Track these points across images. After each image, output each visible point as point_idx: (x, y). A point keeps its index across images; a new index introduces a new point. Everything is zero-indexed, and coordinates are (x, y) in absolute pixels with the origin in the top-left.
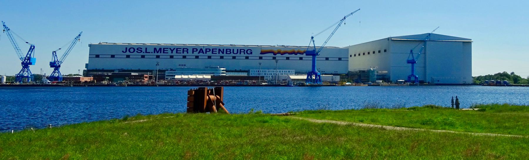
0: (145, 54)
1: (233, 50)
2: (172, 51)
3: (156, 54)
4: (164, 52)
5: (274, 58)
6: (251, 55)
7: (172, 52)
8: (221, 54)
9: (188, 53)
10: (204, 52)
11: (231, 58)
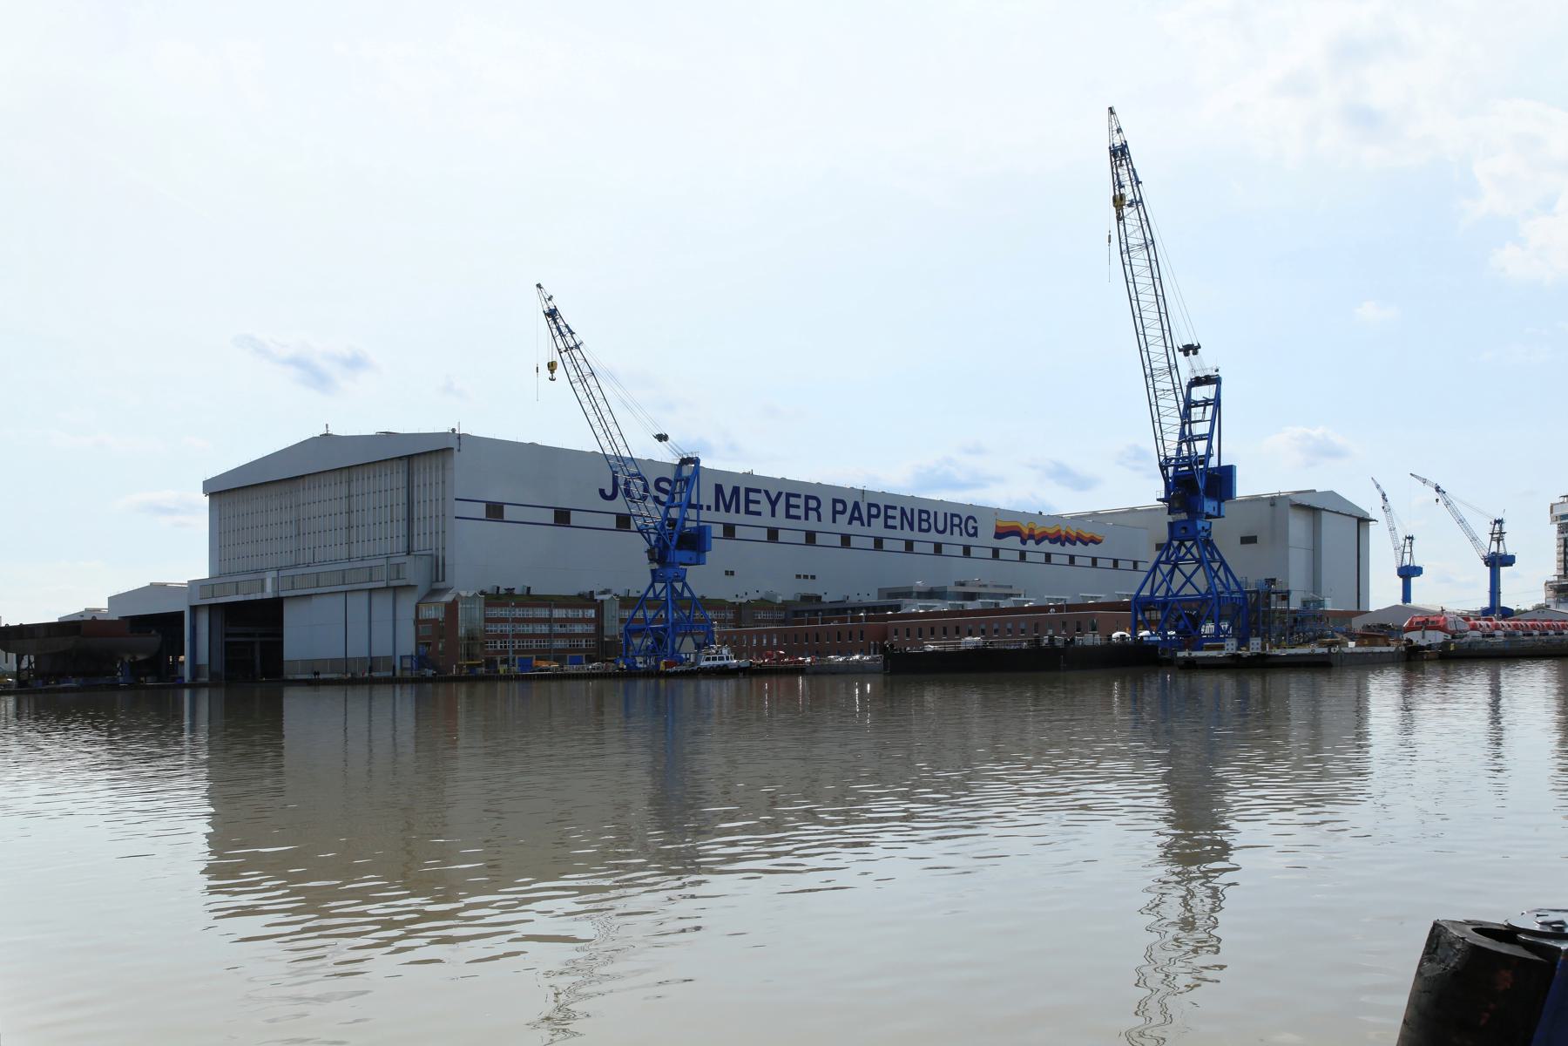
2: (773, 504)
7: (773, 515)
8: (907, 534)
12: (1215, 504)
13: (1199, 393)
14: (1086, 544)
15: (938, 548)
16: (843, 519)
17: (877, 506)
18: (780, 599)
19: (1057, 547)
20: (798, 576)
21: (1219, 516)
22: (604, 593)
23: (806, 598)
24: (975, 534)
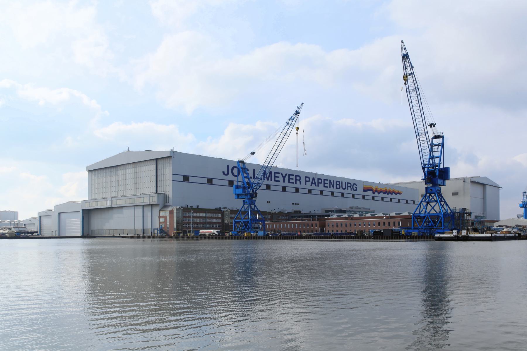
2: (284, 178)
4: (275, 180)
7: (284, 182)
9: (300, 184)
12: (442, 181)
13: (437, 141)
14: (396, 194)
15: (343, 195)
16: (309, 184)
17: (321, 179)
18: (286, 212)
19: (385, 195)
20: (293, 204)
21: (444, 185)
22: (224, 208)
23: (296, 212)
24: (356, 190)
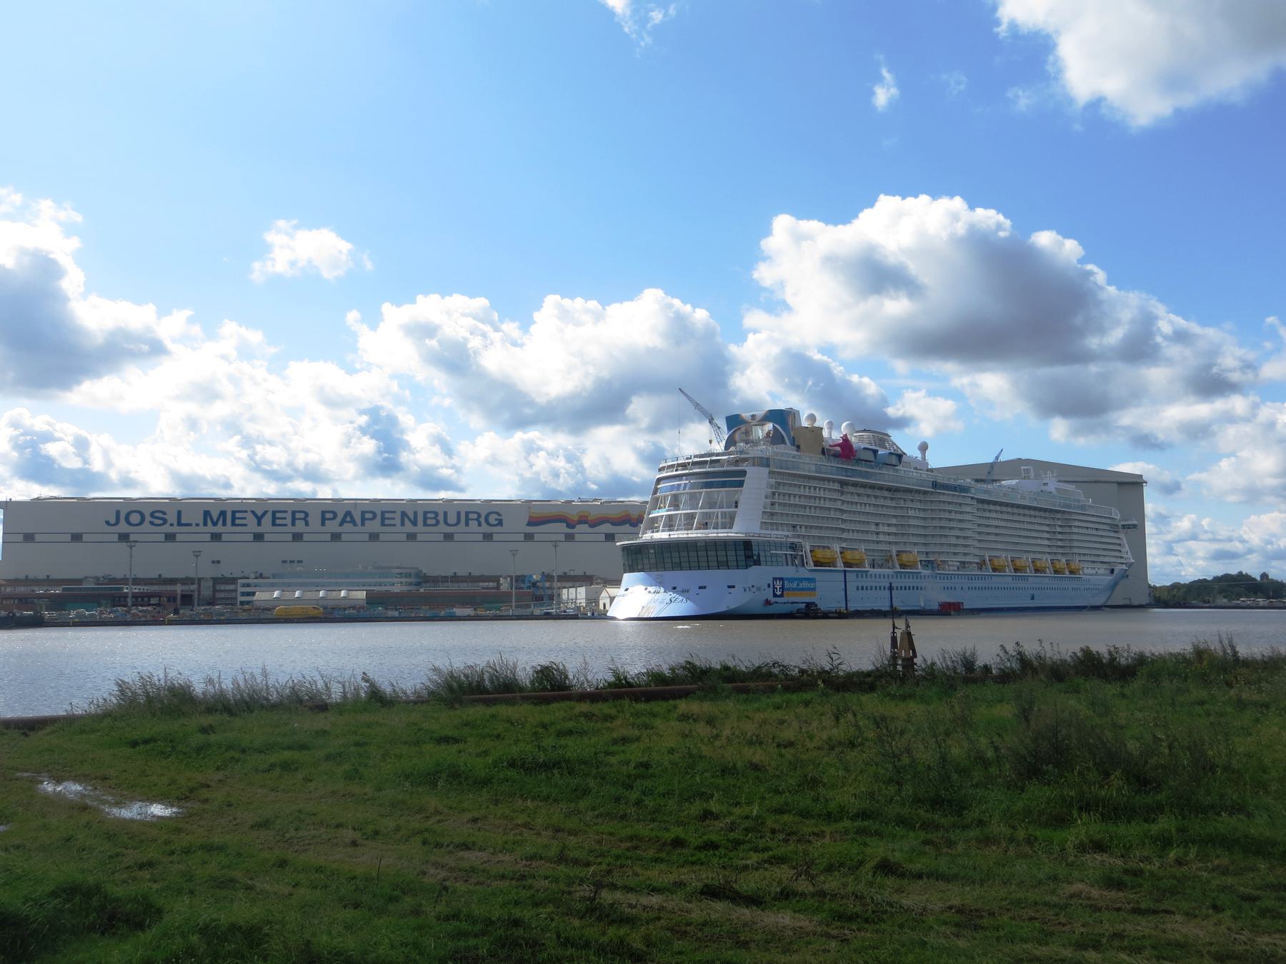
0: (176, 529)
1: (445, 513)
2: (259, 520)
3: (211, 528)
4: (233, 524)
5: (570, 537)
6: (498, 529)
7: (259, 524)
8: (409, 527)
9: (307, 524)
10: (358, 521)
11: (441, 537)
20: (284, 562)
